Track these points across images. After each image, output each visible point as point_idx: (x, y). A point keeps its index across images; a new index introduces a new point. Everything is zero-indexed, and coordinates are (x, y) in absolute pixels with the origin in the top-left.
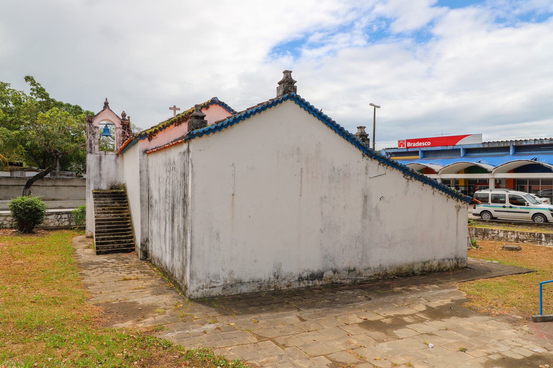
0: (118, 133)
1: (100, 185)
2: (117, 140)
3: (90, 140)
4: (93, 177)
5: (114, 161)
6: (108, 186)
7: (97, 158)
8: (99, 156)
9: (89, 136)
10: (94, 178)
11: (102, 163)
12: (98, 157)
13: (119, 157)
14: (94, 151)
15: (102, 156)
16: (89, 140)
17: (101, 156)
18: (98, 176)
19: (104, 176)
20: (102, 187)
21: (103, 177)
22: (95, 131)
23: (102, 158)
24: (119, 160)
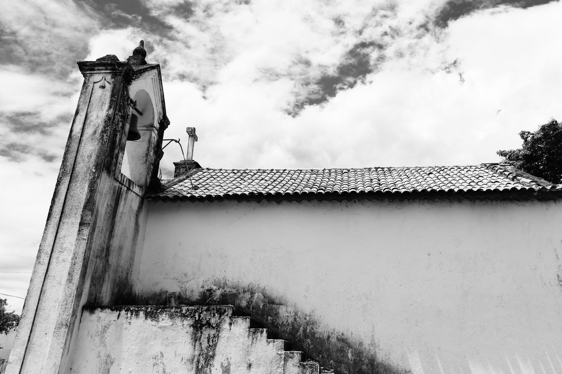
1: (101, 286)
11: (118, 210)
12: (116, 191)
17: (121, 188)
19: (113, 260)
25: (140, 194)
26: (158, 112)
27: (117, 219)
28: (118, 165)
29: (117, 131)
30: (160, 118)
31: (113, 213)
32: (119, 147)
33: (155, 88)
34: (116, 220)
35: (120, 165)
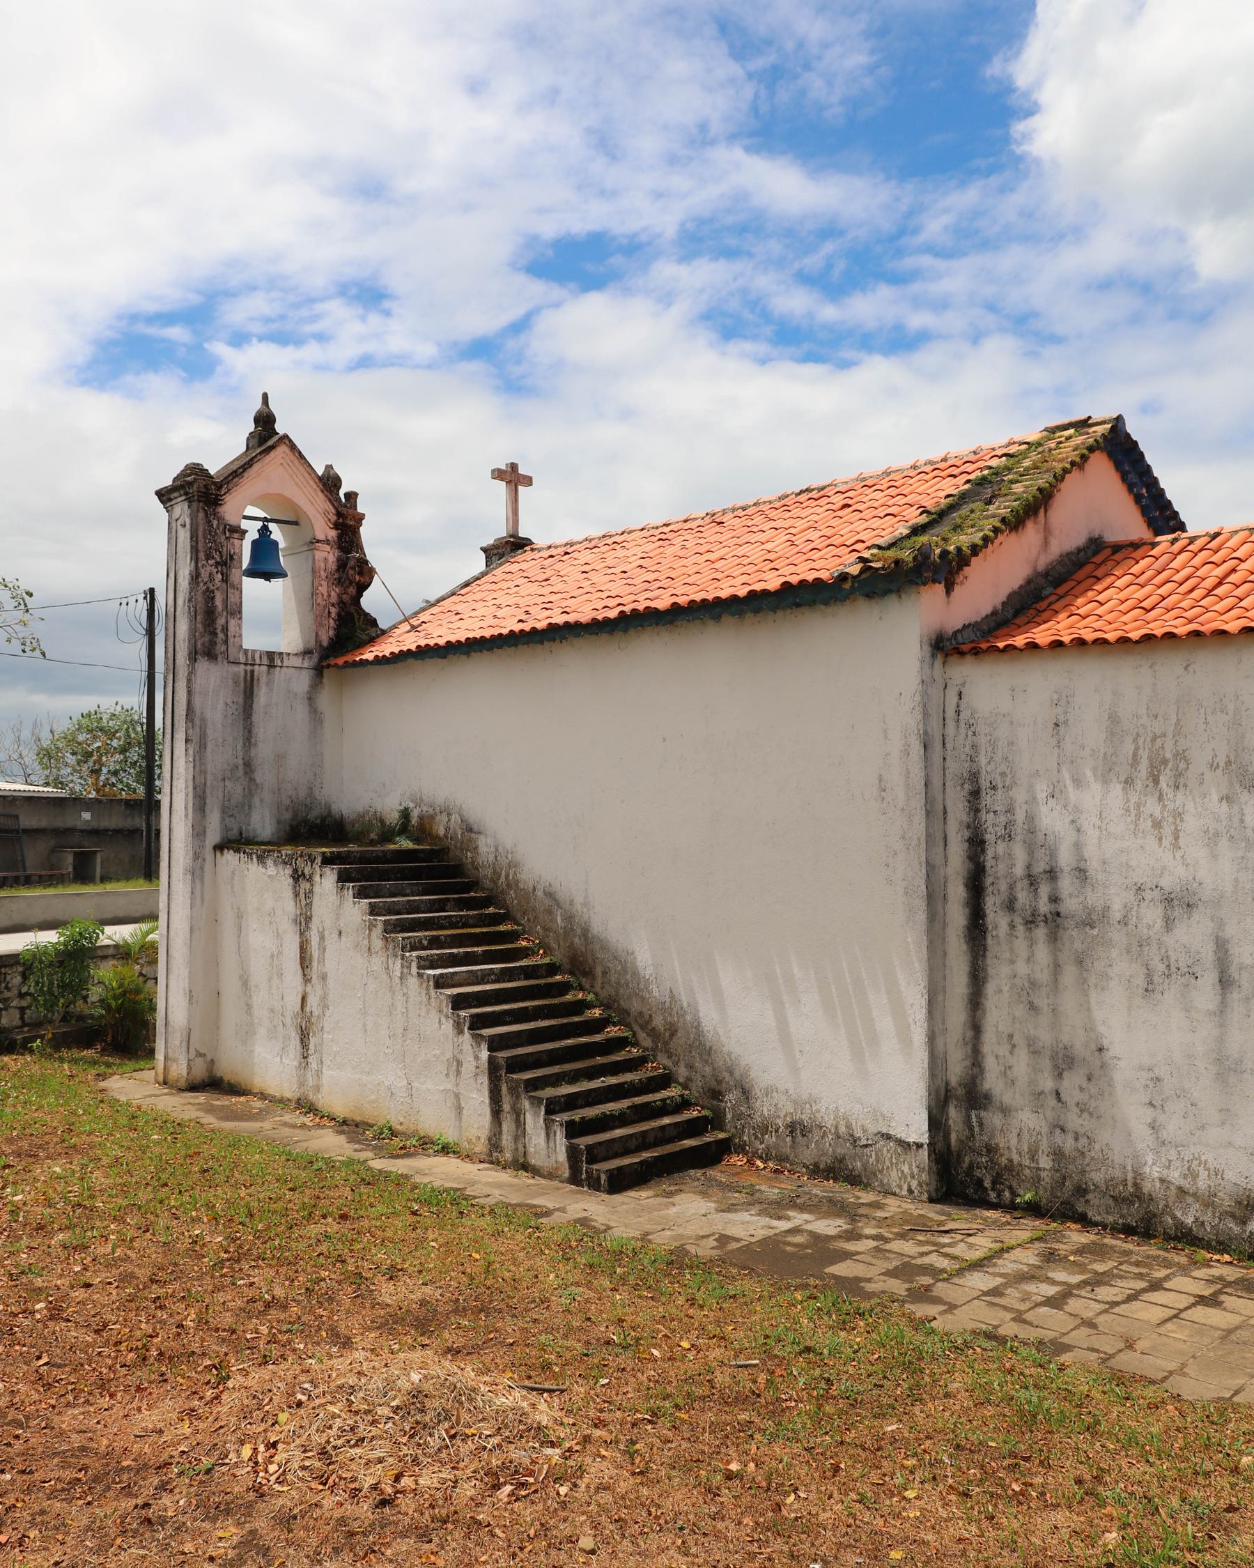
1: (249, 815)
2: (319, 601)
4: (220, 778)
5: (306, 702)
6: (279, 822)
7: (236, 683)
8: (242, 674)
10: (222, 784)
11: (255, 706)
12: (242, 679)
14: (223, 648)
15: (256, 674)
17: (252, 672)
18: (241, 772)
19: (265, 775)
20: (255, 830)
21: (258, 777)
23: (255, 682)
24: (325, 700)
25: (306, 665)
27: (258, 716)
28: (231, 640)
29: (213, 592)
35: (237, 639)
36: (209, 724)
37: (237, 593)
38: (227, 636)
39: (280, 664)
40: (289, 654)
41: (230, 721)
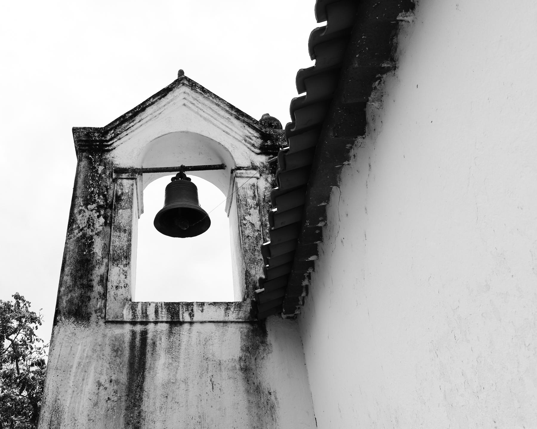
0: (250, 193)
2: (248, 232)
3: (84, 236)
5: (240, 375)
7: (117, 351)
8: (128, 338)
9: (79, 217)
11: (147, 385)
12: (127, 345)
13: (270, 338)
14: (100, 304)
15: (150, 336)
16: (78, 240)
17: (144, 334)
22: (114, 189)
23: (149, 348)
26: (240, 138)
28: (111, 292)
30: (253, 145)
31: (128, 395)
32: (106, 260)
33: (201, 113)
34: (144, 408)
35: (121, 291)
36: (66, 417)
37: (124, 236)
38: (106, 288)
39: (187, 318)
40: (202, 304)
41: (103, 412)
